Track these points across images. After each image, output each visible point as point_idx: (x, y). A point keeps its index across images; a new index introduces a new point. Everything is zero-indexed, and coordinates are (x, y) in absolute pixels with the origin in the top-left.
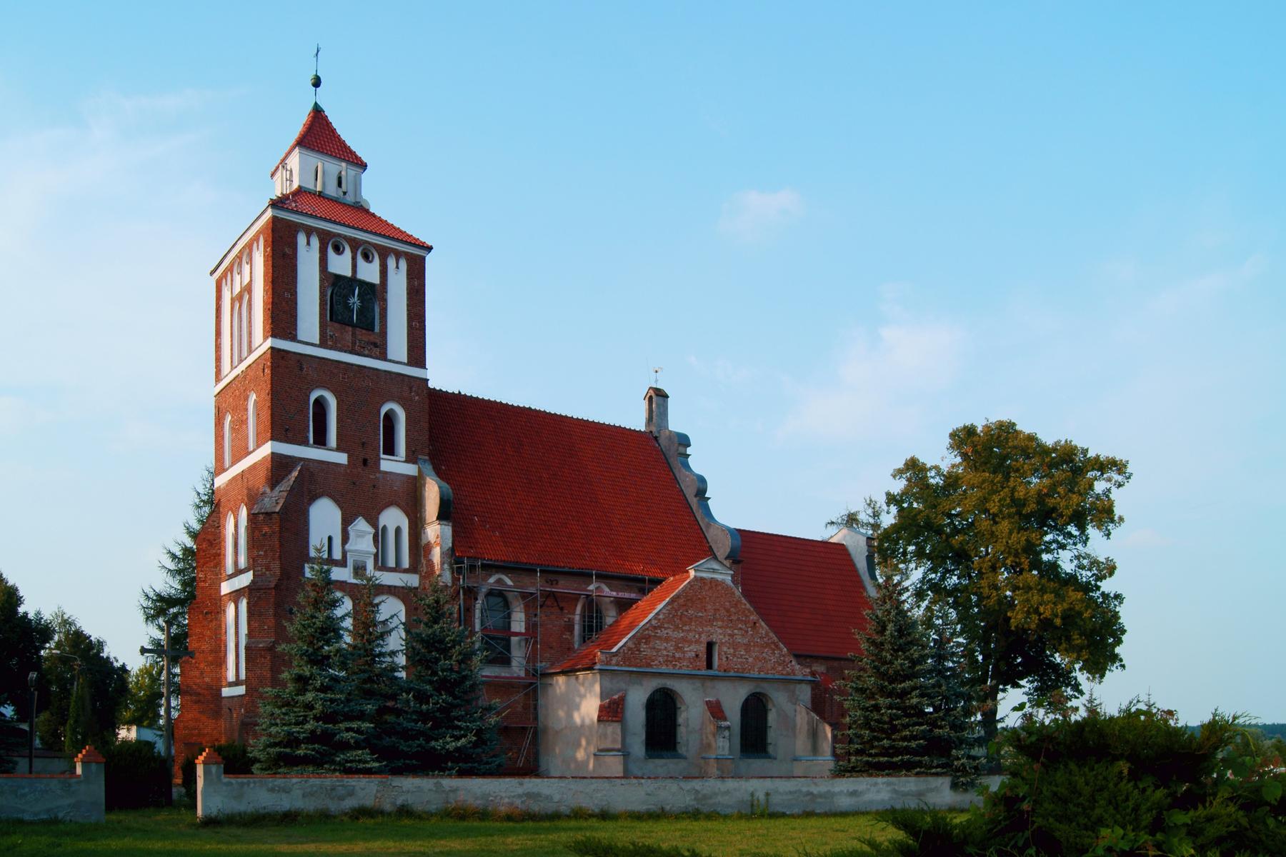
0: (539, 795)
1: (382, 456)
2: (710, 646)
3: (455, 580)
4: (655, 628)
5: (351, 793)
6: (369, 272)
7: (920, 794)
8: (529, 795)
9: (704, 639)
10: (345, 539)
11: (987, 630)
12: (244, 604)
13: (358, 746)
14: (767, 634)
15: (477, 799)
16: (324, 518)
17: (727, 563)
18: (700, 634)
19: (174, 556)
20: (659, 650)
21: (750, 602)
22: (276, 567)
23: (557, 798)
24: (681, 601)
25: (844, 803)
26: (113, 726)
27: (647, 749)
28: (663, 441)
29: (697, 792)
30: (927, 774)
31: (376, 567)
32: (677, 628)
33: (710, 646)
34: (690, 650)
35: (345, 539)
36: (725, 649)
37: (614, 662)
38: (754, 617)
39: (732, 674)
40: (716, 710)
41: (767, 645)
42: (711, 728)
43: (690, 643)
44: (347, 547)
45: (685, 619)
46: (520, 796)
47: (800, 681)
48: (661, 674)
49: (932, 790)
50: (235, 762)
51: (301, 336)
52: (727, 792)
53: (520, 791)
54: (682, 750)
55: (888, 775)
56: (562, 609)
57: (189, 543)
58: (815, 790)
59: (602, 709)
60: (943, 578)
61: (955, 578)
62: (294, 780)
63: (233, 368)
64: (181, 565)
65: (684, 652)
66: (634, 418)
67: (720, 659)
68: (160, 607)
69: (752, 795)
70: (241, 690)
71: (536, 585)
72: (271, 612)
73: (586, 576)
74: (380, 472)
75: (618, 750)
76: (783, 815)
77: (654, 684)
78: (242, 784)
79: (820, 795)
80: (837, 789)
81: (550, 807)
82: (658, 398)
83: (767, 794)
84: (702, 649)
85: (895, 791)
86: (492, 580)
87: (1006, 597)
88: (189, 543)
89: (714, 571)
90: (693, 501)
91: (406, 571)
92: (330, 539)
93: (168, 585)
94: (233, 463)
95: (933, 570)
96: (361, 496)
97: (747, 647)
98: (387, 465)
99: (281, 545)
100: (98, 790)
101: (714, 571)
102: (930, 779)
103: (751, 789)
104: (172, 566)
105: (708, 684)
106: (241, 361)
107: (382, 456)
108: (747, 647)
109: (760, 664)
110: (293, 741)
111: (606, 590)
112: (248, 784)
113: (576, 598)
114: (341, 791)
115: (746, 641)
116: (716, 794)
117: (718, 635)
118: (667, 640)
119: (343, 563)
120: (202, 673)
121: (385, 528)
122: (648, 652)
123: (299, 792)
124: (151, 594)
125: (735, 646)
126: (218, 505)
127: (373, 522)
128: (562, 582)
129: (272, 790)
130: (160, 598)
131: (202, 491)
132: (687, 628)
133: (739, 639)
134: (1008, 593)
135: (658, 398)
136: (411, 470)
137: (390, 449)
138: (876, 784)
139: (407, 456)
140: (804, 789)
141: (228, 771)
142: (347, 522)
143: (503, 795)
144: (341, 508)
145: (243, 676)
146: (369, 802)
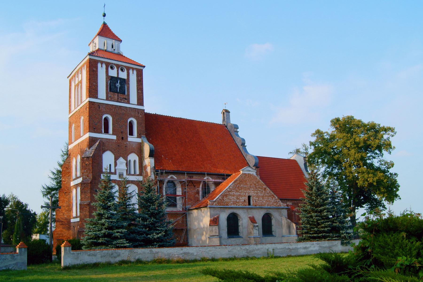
0: (188, 253)
1: (129, 136)
2: (249, 197)
3: (156, 178)
4: (229, 192)
5: (119, 255)
7: (330, 247)
8: (185, 253)
9: (247, 195)
10: (116, 165)
11: (349, 187)
12: (79, 189)
13: (121, 238)
14: (270, 192)
15: (166, 255)
16: (108, 158)
17: (254, 168)
18: (245, 193)
19: (54, 173)
21: (263, 181)
23: (195, 254)
24: (238, 182)
25: (302, 251)
26: (30, 234)
28: (229, 127)
29: (247, 250)
30: (332, 240)
31: (127, 174)
32: (237, 191)
33: (249, 197)
34: (242, 199)
35: (116, 165)
36: (255, 198)
37: (214, 204)
38: (265, 186)
39: (258, 207)
40: (253, 220)
41: (270, 196)
42: (251, 226)
43: (242, 196)
44: (116, 168)
45: (240, 188)
46: (181, 254)
47: (283, 208)
48: (232, 208)
49: (334, 246)
50: (76, 246)
52: (258, 249)
53: (182, 252)
54: (241, 235)
55: (317, 241)
56: (195, 186)
57: (59, 168)
58: (291, 247)
59: (211, 221)
60: (332, 170)
61: (336, 170)
62: (98, 251)
64: (56, 176)
65: (240, 200)
66: (218, 120)
67: (253, 202)
68: (49, 191)
69: (268, 250)
70: (78, 220)
71: (185, 178)
72: (89, 191)
73: (203, 174)
74: (128, 141)
75: (218, 236)
76: (280, 257)
77: (229, 212)
78: (78, 254)
79: (293, 249)
80: (299, 247)
81: (193, 258)
82: (226, 112)
83: (273, 250)
85: (320, 247)
86: (169, 177)
87: (355, 176)
88: (59, 168)
89: (249, 171)
90: (241, 147)
91: (138, 175)
92: (110, 165)
93: (52, 184)
94: (75, 141)
95: (328, 167)
96: (121, 150)
97: (263, 197)
98: (130, 139)
99: (93, 168)
100: (25, 258)
101: (249, 171)
102: (333, 241)
103: (267, 248)
104: (53, 177)
105: (249, 211)
107: (129, 136)
108: (263, 197)
109: (268, 203)
110: (97, 237)
111: (211, 179)
112: (81, 253)
113: (200, 182)
114: (115, 255)
115: (262, 195)
116: (254, 250)
117: (252, 193)
118: (234, 195)
119: (115, 173)
120: (64, 214)
121: (130, 161)
122: (227, 200)
123: (100, 256)
124: (45, 187)
125: (258, 197)
126: (70, 155)
127: (126, 159)
128: (194, 177)
129: (89, 255)
130: (49, 188)
131: (64, 150)
132: (241, 191)
133: (260, 194)
134: (356, 174)
135: (226, 112)
136: (139, 140)
137: (131, 134)
138: (313, 244)
140: (287, 247)
141: (73, 249)
142: (116, 159)
143: (176, 254)
144: (114, 154)
145: (79, 215)
146: (126, 258)
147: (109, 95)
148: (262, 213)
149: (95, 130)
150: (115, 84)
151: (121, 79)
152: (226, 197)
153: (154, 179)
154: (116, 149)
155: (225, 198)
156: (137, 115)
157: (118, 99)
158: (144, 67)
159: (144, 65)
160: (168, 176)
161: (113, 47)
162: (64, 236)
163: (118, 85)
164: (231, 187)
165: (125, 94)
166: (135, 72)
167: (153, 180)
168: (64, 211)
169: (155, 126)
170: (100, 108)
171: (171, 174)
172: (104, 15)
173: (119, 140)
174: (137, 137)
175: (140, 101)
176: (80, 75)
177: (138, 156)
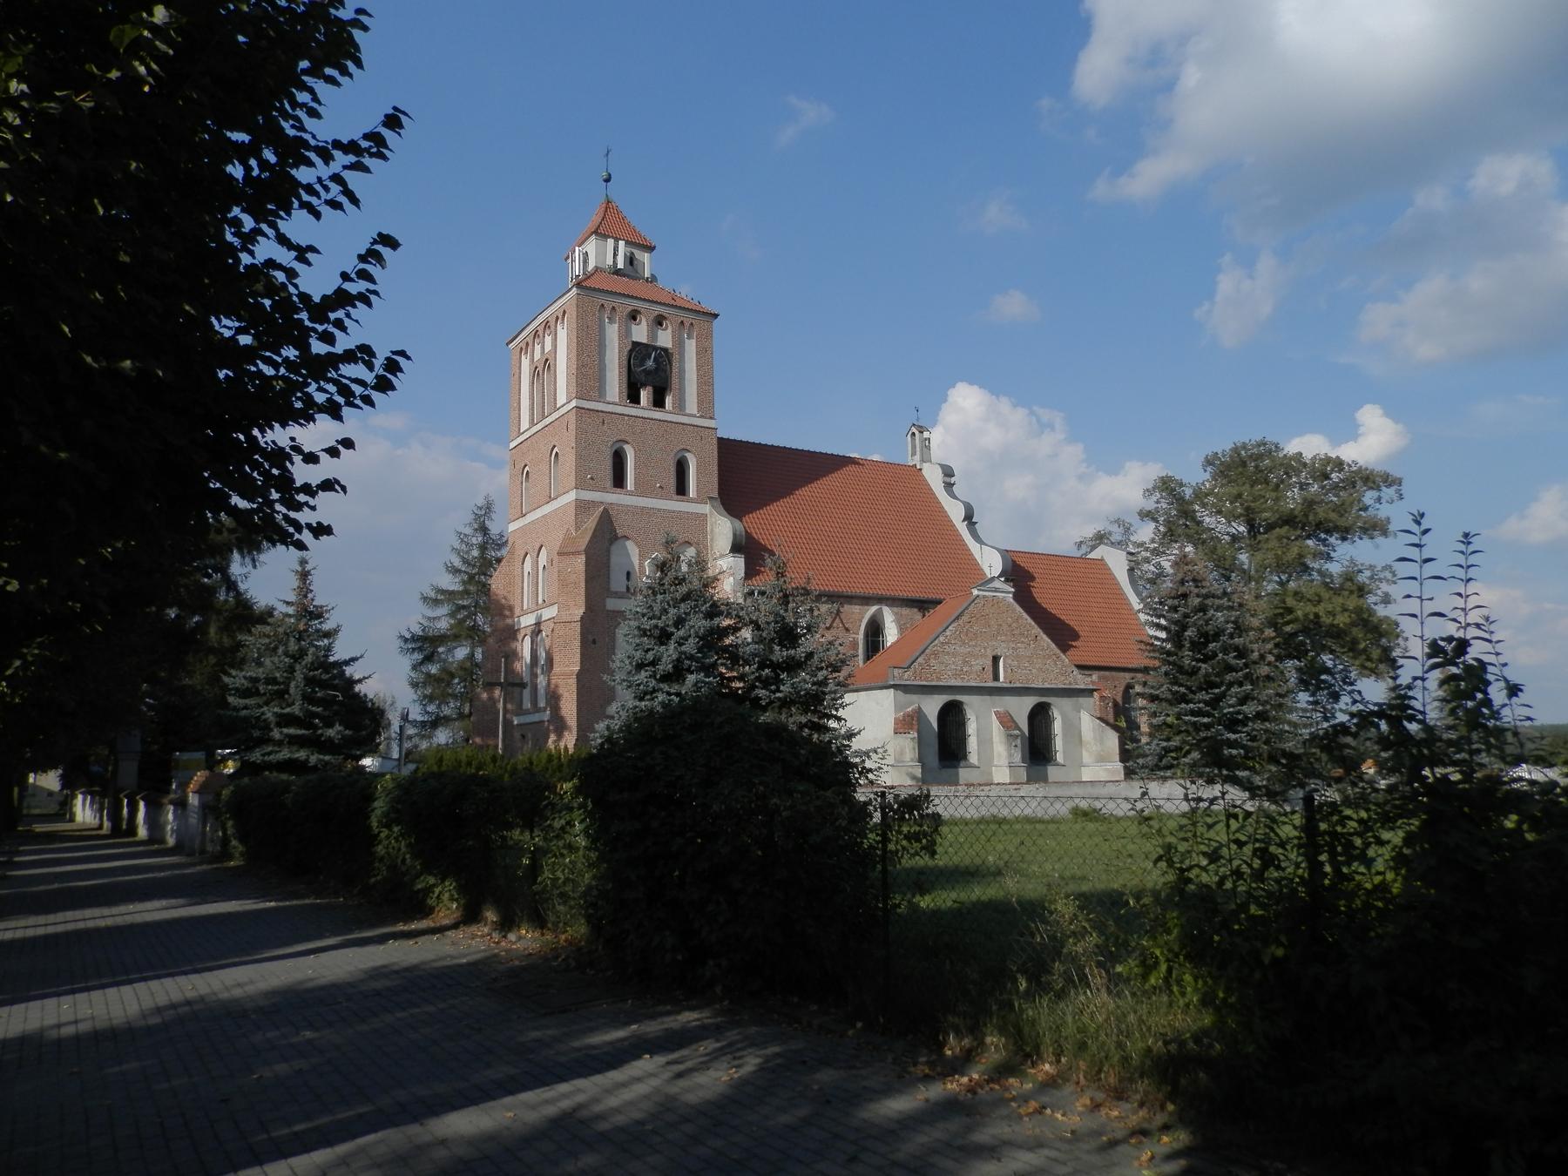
6: (665, 339)
9: (990, 654)
21: (1034, 618)
33: (996, 659)
51: (608, 399)
59: (897, 722)
63: (532, 424)
84: (989, 662)
90: (962, 528)
106: (544, 417)
118: (954, 655)
148: (1029, 702)
151: (655, 348)
158: (716, 316)
163: (650, 363)
164: (948, 633)
175: (707, 405)
176: (548, 340)
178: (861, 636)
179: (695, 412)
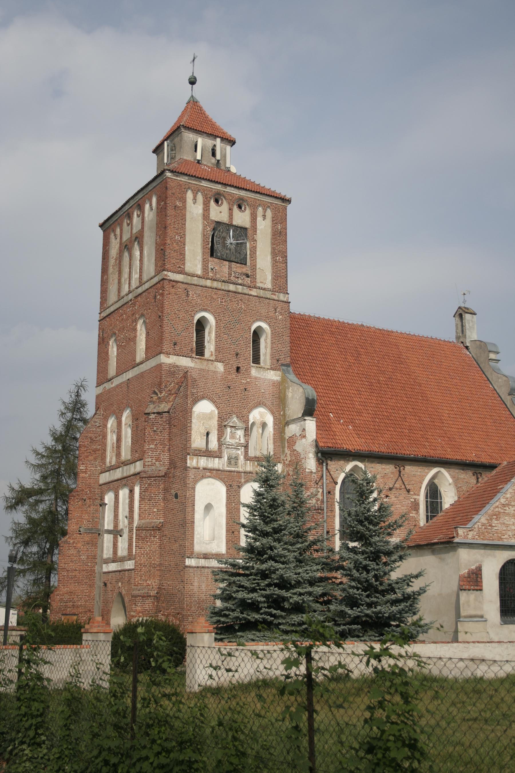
20: (507, 526)
22: (165, 457)
27: (502, 615)
37: (470, 536)
72: (161, 496)
94: (118, 375)
99: (170, 440)
107: (252, 364)
122: (499, 527)
139: (272, 364)
147: (210, 266)
149: (177, 348)
150: (224, 238)
152: (497, 519)
153: (314, 471)
154: (223, 395)
155: (495, 522)
156: (271, 314)
157: (230, 274)
158: (289, 201)
159: (288, 197)
160: (348, 463)
161: (214, 154)
162: (78, 607)
164: (508, 496)
165: (246, 264)
166: (269, 213)
167: (311, 472)
168: (79, 545)
169: (312, 344)
170: (188, 295)
171: (354, 460)
172: (193, 82)
173: (230, 373)
174: (272, 369)
177: (273, 413)
178: (422, 498)
179: (269, 285)
